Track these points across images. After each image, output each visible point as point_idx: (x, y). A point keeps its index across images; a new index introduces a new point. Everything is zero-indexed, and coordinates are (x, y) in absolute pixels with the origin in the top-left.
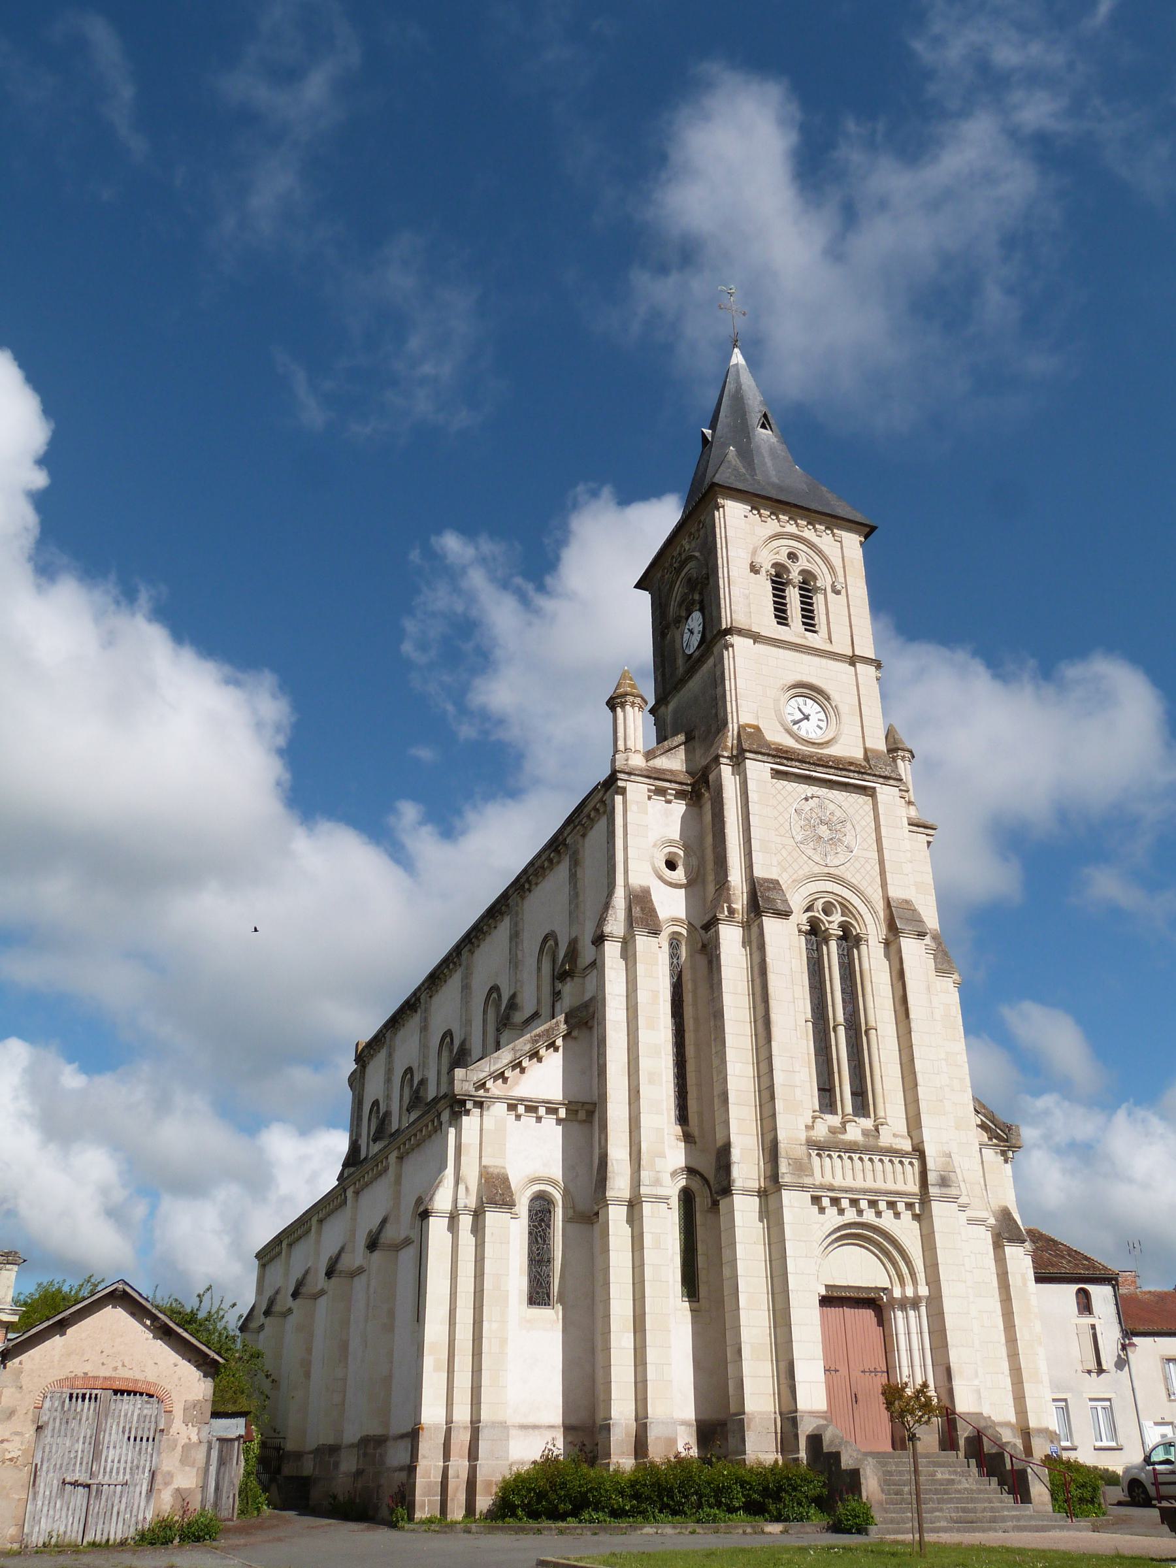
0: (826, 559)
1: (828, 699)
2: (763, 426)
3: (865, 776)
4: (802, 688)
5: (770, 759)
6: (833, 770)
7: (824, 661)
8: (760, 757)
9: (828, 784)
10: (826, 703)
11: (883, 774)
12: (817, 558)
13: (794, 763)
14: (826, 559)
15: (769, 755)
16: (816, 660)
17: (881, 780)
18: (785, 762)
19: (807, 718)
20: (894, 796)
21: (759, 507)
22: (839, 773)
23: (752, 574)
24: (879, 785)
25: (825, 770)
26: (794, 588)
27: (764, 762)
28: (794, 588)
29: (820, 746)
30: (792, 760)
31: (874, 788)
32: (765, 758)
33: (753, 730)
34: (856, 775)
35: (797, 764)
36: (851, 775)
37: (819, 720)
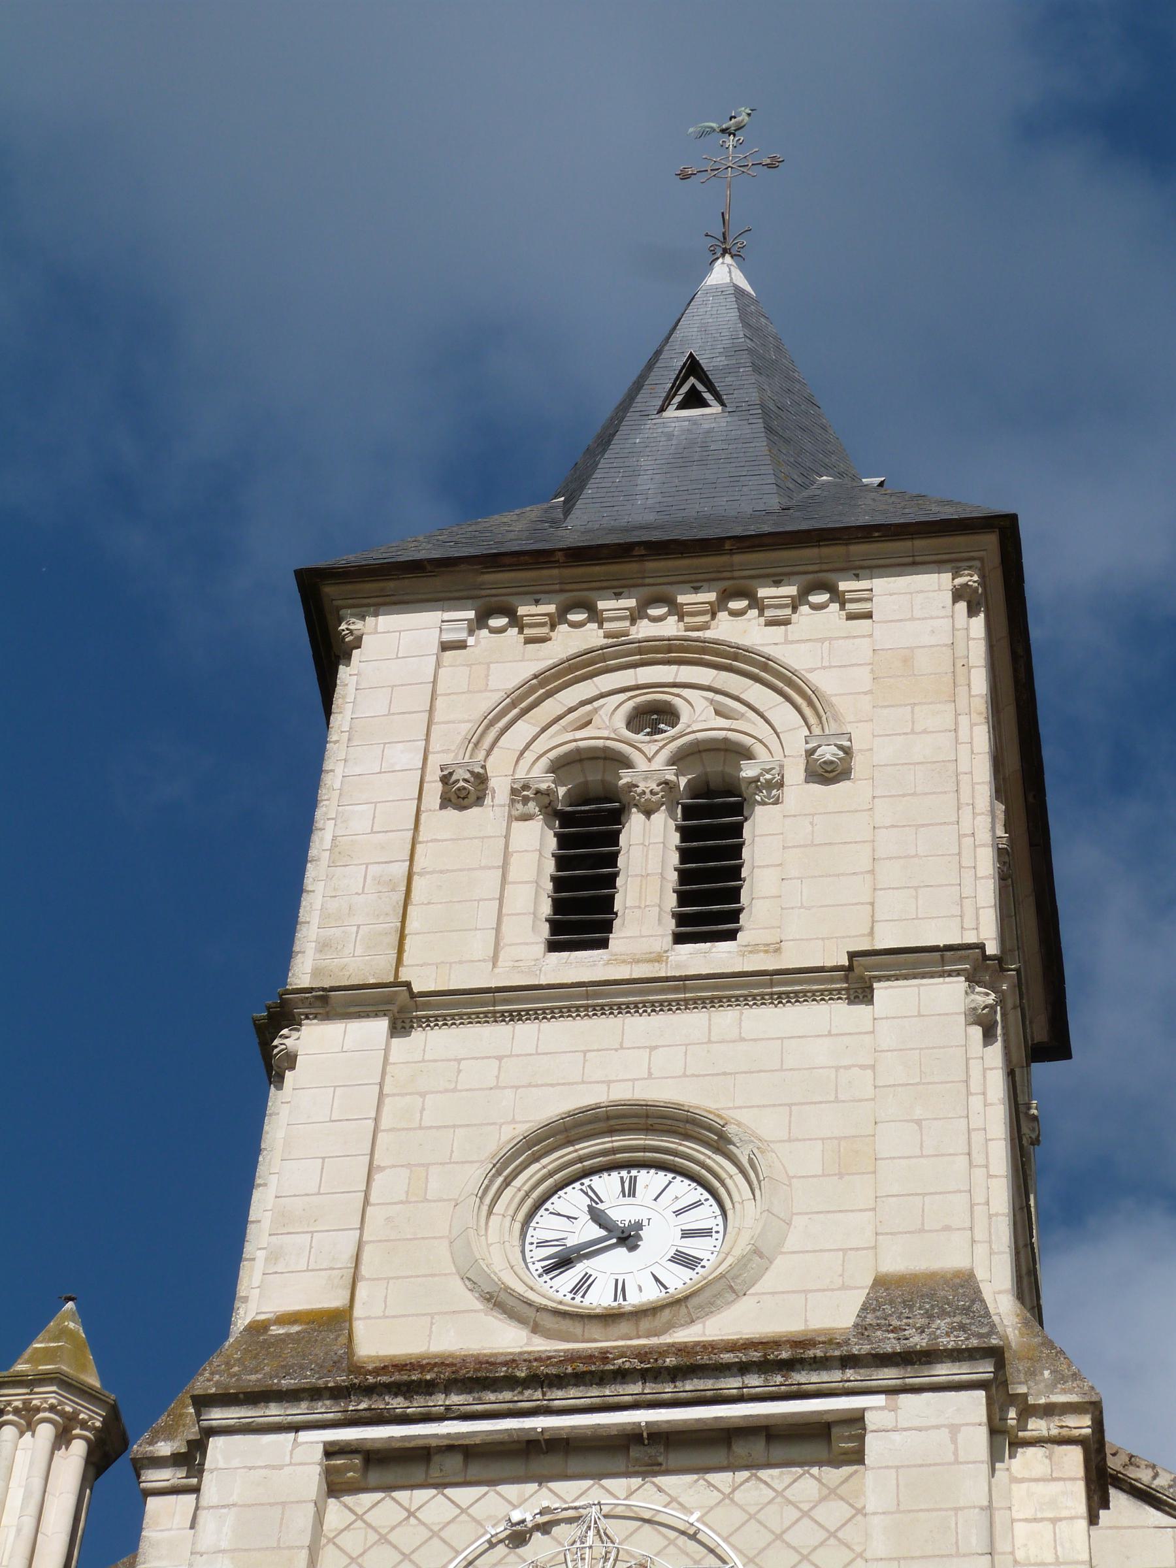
0: (790, 683)
1: (720, 1142)
2: (693, 400)
3: (801, 1378)
4: (611, 1132)
5: (324, 1410)
6: (636, 1388)
7: (725, 1019)
8: (274, 1412)
9: (635, 1452)
10: (719, 1162)
11: (891, 1345)
12: (756, 693)
13: (439, 1401)
14: (790, 683)
15: (314, 1394)
16: (693, 1021)
17: (888, 1375)
18: (397, 1404)
19: (628, 1238)
20: (954, 1429)
21: (513, 600)
22: (668, 1390)
23: (451, 813)
24: (879, 1400)
25: (594, 1394)
26: (648, 813)
27: (296, 1428)
28: (648, 813)
29: (645, 1324)
30: (428, 1388)
31: (856, 1419)
32: (298, 1412)
33: (295, 1329)
34: (754, 1381)
35: (455, 1399)
36: (731, 1384)
37: (687, 1234)
